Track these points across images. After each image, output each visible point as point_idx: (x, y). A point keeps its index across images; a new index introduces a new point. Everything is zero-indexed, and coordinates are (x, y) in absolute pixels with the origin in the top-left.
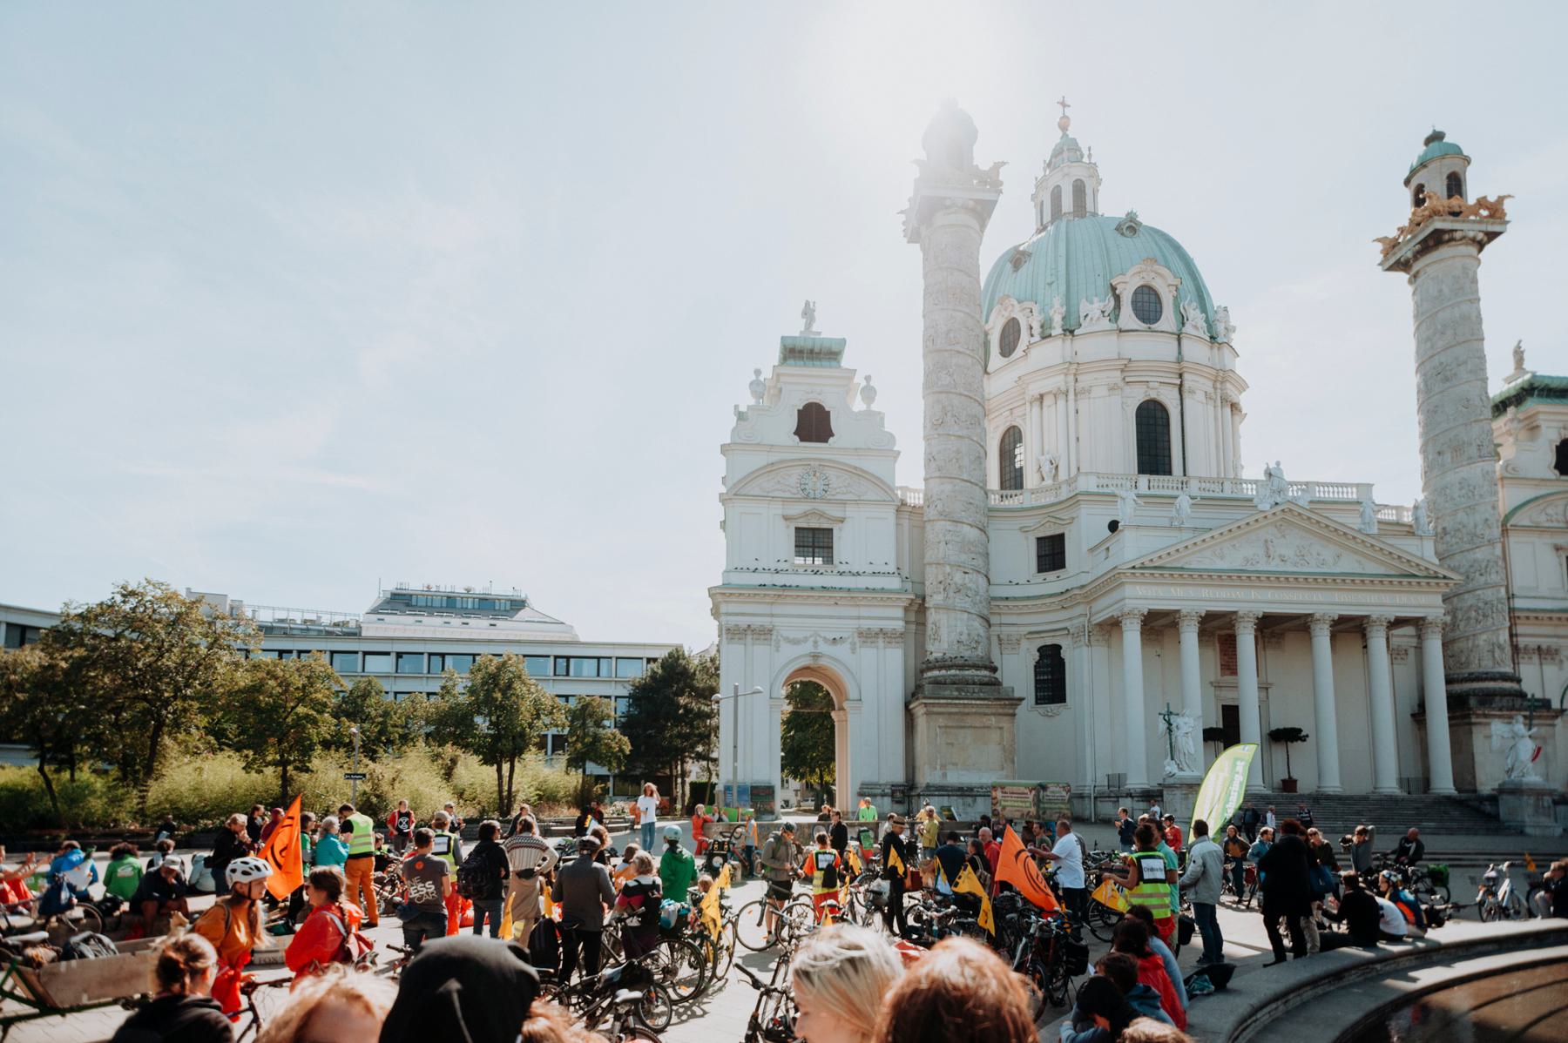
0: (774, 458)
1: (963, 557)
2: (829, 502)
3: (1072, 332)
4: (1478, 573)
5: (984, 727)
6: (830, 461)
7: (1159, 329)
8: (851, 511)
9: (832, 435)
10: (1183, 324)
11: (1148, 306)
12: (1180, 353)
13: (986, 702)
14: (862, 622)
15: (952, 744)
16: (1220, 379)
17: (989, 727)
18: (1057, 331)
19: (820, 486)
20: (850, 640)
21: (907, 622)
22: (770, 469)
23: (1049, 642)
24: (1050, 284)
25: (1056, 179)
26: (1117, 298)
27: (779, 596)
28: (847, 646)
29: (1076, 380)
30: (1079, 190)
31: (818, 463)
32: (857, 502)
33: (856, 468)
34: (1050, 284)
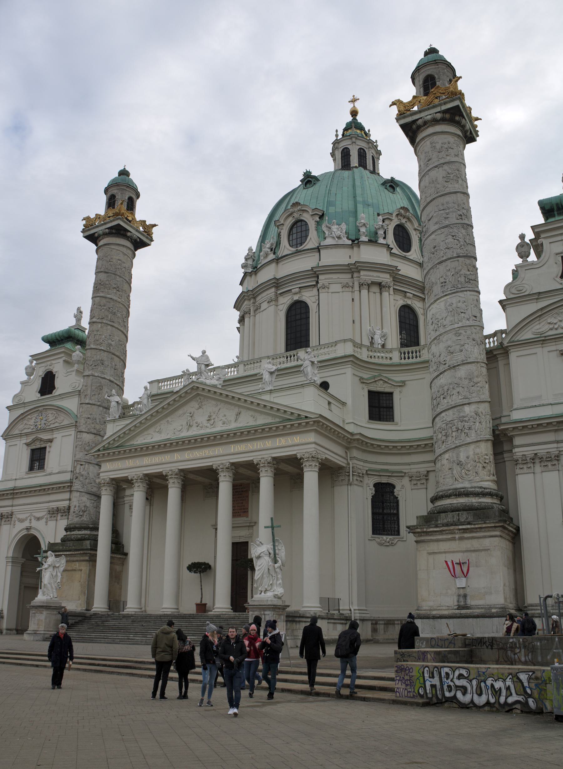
1: (81, 454)
4: (442, 397)
5: (72, 570)
7: (304, 249)
9: (54, 388)
10: (325, 238)
12: (320, 260)
13: (71, 553)
14: (51, 504)
16: (353, 270)
17: (75, 570)
19: (43, 422)
20: (46, 517)
26: (279, 235)
27: (13, 493)
28: (44, 520)
30: (346, 154)
31: (42, 408)
32: (57, 429)
33: (58, 407)
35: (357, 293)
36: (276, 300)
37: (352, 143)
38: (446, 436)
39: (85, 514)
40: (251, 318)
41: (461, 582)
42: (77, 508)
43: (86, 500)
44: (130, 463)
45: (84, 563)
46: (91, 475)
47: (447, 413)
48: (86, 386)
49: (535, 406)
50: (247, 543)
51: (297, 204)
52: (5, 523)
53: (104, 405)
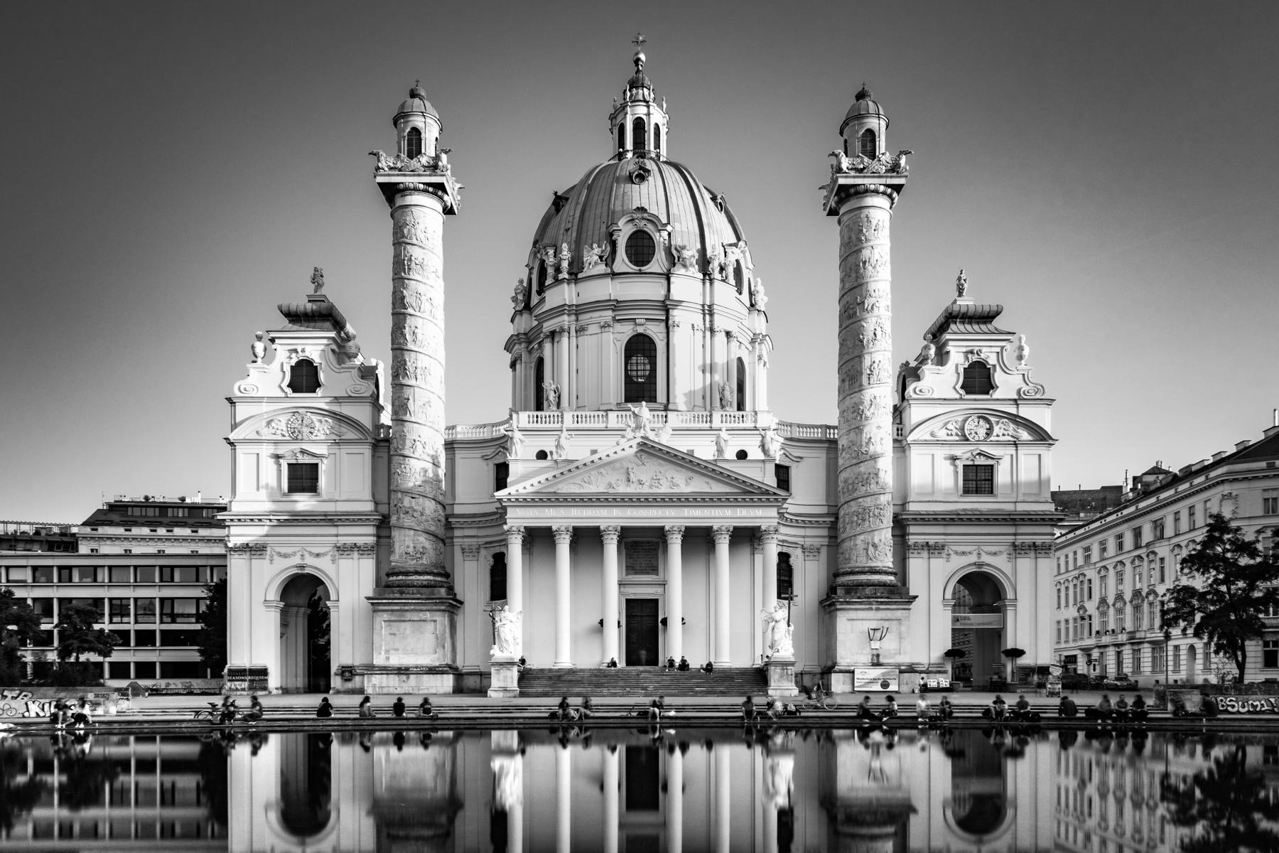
3: (576, 275)
10: (674, 265)
11: (641, 248)
12: (669, 290)
14: (340, 538)
15: (395, 634)
18: (565, 275)
20: (331, 553)
21: (378, 537)
23: (498, 550)
28: (328, 558)
36: (613, 327)
37: (648, 114)
39: (425, 557)
41: (876, 645)
42: (411, 550)
43: (424, 541)
45: (439, 613)
46: (427, 512)
47: (865, 499)
49: (929, 501)
50: (657, 601)
52: (255, 557)
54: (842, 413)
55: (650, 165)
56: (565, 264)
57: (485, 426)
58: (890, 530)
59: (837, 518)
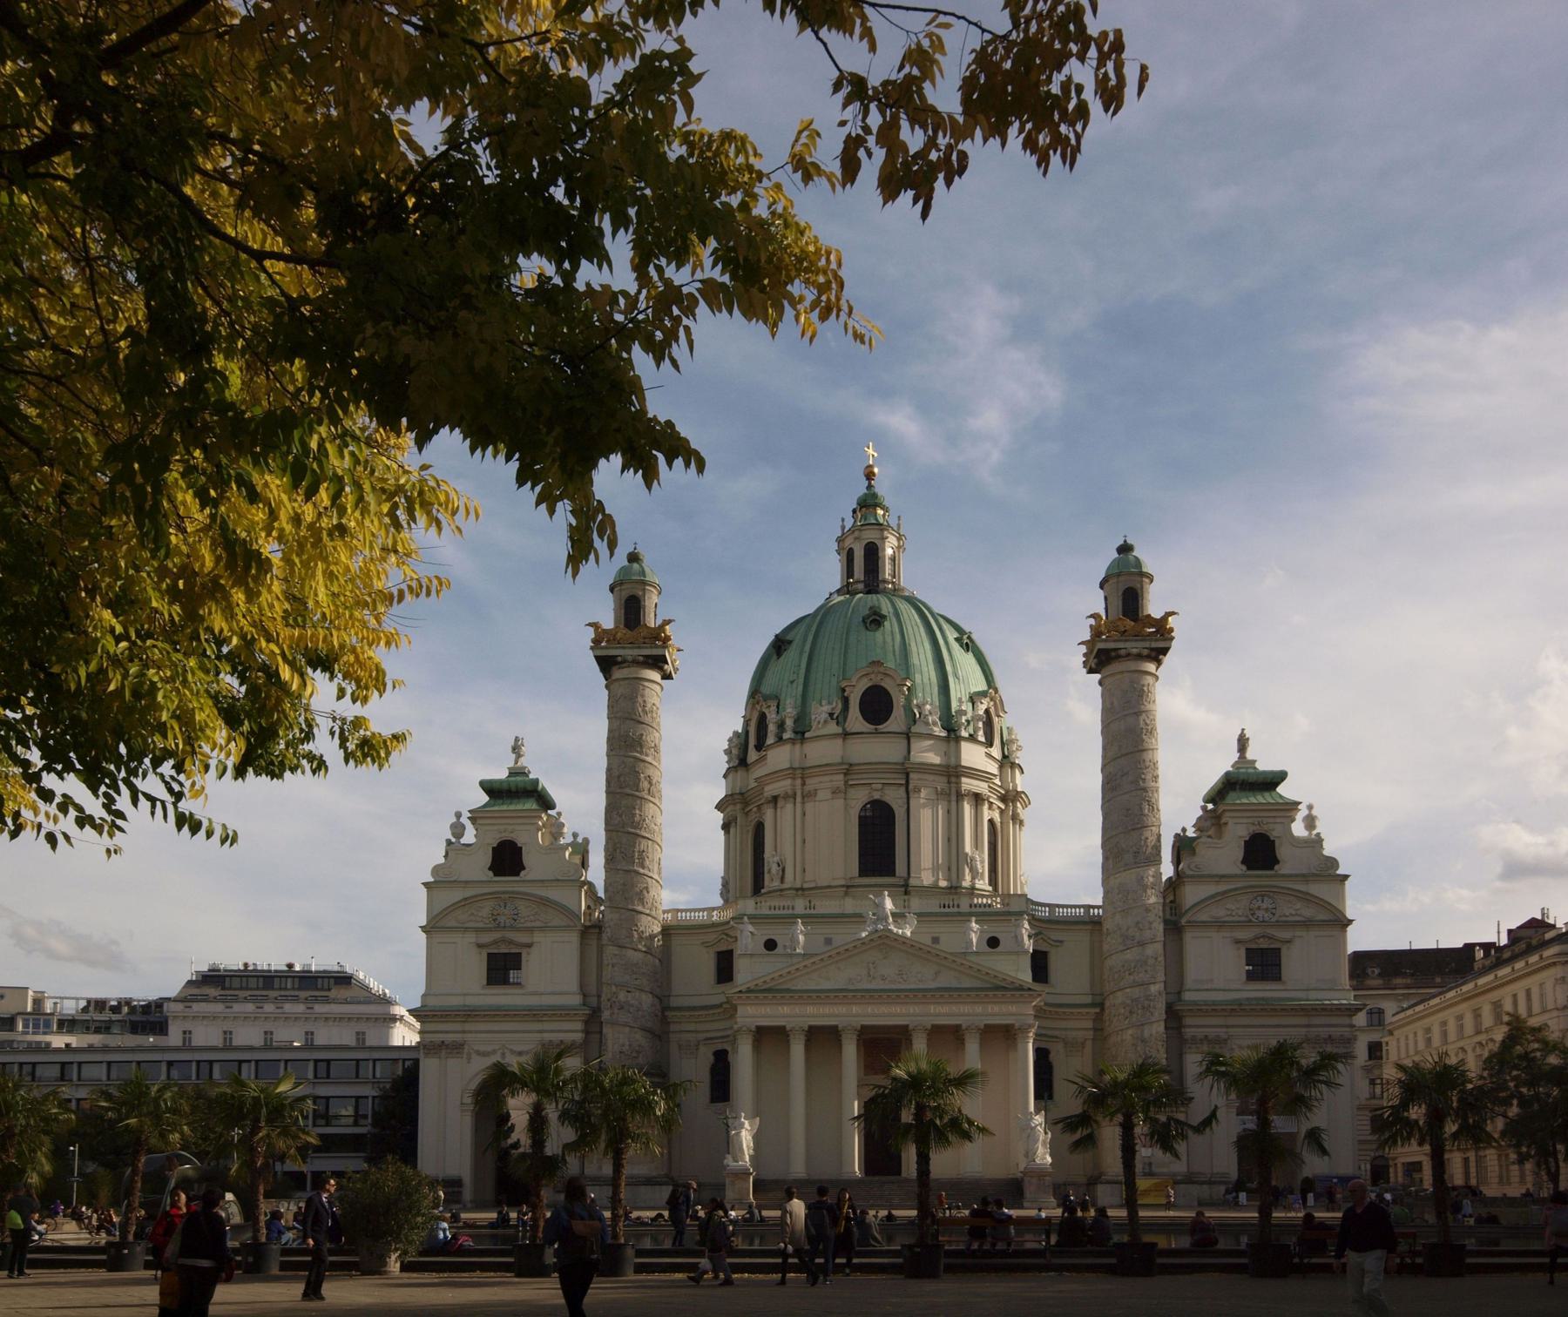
0: (469, 892)
2: (518, 930)
3: (803, 733)
6: (518, 893)
8: (538, 937)
9: (524, 868)
11: (877, 705)
12: (909, 752)
22: (465, 903)
24: (792, 682)
25: (848, 543)
26: (846, 701)
29: (804, 784)
30: (873, 553)
32: (542, 929)
33: (541, 898)
34: (792, 682)
35: (954, 804)
37: (884, 539)
38: (1131, 1012)
40: (799, 805)
44: (786, 1010)
48: (624, 885)
51: (878, 663)
53: (653, 913)
54: (1106, 894)
55: (885, 607)
56: (789, 723)
57: (703, 910)
58: (1162, 1024)
59: (1103, 1010)
